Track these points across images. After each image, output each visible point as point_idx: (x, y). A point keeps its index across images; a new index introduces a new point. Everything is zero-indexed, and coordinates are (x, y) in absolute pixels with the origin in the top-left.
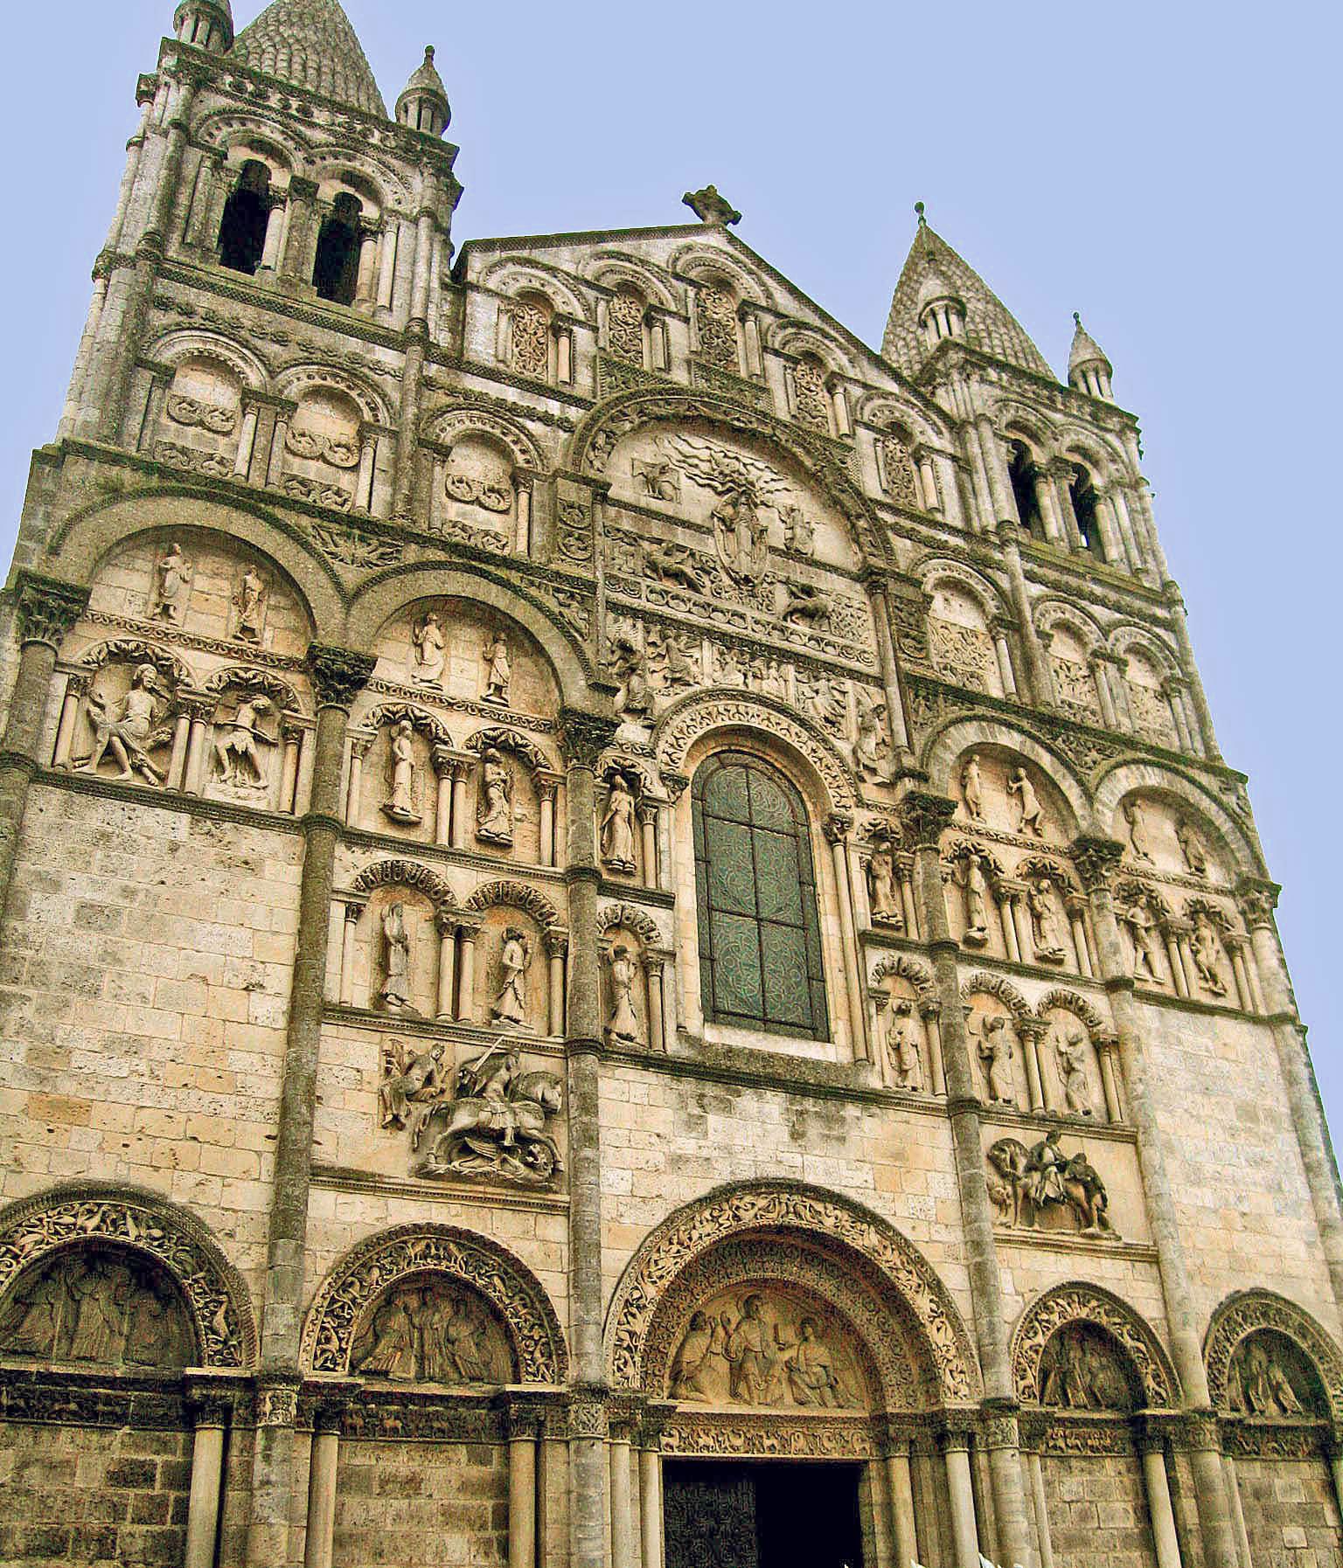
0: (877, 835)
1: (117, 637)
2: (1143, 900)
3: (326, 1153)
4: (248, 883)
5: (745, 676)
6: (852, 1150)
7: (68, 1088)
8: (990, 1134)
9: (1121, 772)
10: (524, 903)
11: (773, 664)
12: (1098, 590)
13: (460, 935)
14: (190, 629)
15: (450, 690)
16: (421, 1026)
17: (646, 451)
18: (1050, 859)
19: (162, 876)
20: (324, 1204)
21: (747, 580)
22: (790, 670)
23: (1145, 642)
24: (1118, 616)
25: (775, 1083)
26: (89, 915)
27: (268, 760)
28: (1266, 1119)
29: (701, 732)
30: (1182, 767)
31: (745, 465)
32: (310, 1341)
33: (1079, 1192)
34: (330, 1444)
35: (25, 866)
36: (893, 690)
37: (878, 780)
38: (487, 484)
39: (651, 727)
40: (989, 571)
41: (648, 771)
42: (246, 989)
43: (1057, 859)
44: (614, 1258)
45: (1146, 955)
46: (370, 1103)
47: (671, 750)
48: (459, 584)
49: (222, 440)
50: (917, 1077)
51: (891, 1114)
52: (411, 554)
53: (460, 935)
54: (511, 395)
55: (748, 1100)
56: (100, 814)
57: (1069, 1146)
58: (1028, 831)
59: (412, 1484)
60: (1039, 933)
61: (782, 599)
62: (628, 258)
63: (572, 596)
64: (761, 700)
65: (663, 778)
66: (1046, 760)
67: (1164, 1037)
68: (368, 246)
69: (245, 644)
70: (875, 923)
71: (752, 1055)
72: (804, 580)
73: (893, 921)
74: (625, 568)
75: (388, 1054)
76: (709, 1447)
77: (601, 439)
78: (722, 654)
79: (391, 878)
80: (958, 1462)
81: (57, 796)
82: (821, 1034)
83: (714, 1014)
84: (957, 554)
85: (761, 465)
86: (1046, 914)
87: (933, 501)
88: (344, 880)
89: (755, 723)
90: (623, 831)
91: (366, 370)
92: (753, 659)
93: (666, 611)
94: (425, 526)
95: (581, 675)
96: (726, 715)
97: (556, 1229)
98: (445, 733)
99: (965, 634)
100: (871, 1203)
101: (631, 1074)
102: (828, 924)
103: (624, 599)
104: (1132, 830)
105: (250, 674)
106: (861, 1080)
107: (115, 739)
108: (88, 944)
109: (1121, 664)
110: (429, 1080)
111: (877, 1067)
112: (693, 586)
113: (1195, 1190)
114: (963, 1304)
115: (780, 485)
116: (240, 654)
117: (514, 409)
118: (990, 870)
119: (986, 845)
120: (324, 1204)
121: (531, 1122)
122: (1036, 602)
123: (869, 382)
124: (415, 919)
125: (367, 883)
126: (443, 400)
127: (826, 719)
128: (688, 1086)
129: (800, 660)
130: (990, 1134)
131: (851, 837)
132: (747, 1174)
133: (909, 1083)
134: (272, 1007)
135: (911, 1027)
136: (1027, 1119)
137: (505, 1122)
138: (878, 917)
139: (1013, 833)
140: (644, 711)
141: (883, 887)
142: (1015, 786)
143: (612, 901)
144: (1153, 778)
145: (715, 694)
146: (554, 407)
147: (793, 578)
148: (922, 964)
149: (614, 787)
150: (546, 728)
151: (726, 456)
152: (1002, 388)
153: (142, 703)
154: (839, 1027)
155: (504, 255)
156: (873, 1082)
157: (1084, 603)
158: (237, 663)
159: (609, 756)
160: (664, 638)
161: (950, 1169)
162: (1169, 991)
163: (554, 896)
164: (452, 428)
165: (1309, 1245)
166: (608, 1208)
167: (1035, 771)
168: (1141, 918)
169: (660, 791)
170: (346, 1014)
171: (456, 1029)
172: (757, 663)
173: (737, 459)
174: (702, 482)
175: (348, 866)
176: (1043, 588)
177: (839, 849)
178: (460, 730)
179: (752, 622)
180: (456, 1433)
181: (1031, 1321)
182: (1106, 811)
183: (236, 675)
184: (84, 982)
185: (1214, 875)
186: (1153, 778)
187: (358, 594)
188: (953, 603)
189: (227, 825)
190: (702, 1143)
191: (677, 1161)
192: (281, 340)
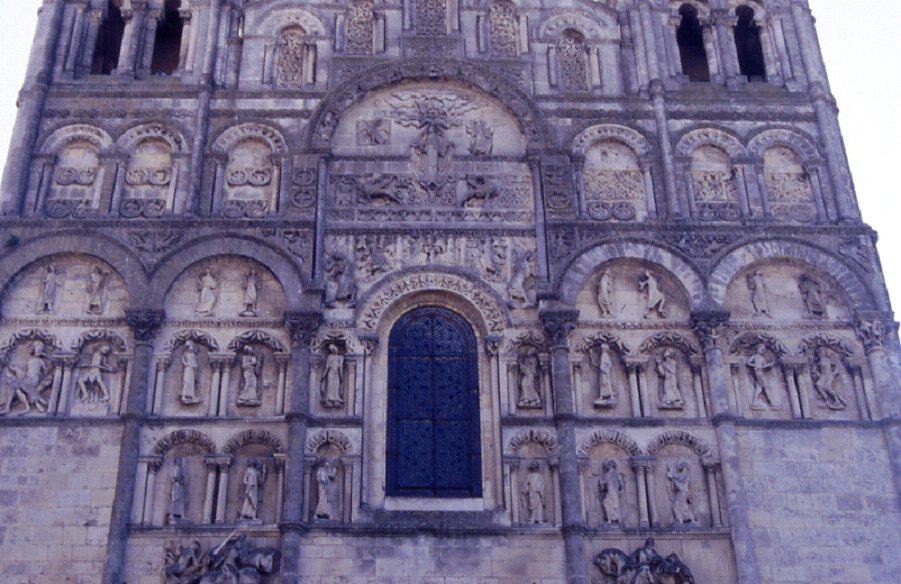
0: (524, 342)
1: (20, 330)
2: (762, 347)
4: (90, 461)
5: (429, 254)
6: (485, 568)
8: (592, 547)
9: (738, 253)
11: (450, 241)
13: (218, 469)
16: (189, 529)
17: (367, 113)
18: (673, 333)
19: (41, 466)
21: (433, 186)
22: (463, 241)
24: (760, 124)
28: (869, 506)
29: (391, 302)
31: (441, 101)
36: (541, 237)
37: (525, 305)
38: (255, 169)
39: (354, 307)
40: (639, 122)
41: (350, 338)
42: (87, 525)
43: (679, 331)
45: (763, 389)
47: (368, 319)
49: (88, 190)
50: (539, 513)
53: (218, 469)
54: (270, 104)
55: (407, 547)
57: (664, 547)
58: (654, 316)
60: (662, 390)
63: (297, 234)
64: (439, 269)
65: (361, 339)
66: (667, 259)
67: (768, 453)
68: (185, 27)
69: (95, 317)
70: (519, 408)
71: (412, 515)
72: (479, 173)
73: (533, 404)
74: (344, 202)
75: (168, 550)
78: (411, 243)
82: (475, 492)
83: (393, 489)
84: (611, 116)
85: (454, 97)
86: (668, 375)
87: (596, 81)
88: (148, 449)
89: (433, 287)
90: (334, 381)
91: (174, 118)
92: (435, 240)
93: (372, 224)
95: (300, 286)
96: (410, 285)
98: (216, 343)
102: (485, 415)
103: (342, 223)
104: (753, 295)
105: (97, 334)
106: (495, 521)
107: (19, 392)
109: (756, 161)
110: (191, 562)
111: (508, 511)
112: (391, 199)
113: (788, 569)
115: (465, 108)
116: (90, 322)
117: (272, 114)
118: (618, 351)
119: (615, 333)
122: (675, 138)
124: (195, 466)
125: (162, 449)
127: (488, 270)
128: (364, 542)
130: (592, 547)
131: (502, 351)
133: (533, 520)
134: (100, 533)
136: (628, 532)
138: (521, 404)
140: (349, 297)
141: (528, 382)
142: (642, 284)
143: (320, 429)
145: (406, 271)
146: (298, 104)
147: (470, 173)
148: (549, 433)
149: (330, 352)
150: (275, 325)
151: (426, 99)
154: (487, 486)
155: (270, 5)
156: (504, 521)
158: (89, 329)
159: (324, 334)
160: (368, 242)
161: (562, 576)
162: (785, 416)
163: (280, 433)
164: (224, 141)
168: (760, 362)
169: (358, 348)
170: (146, 529)
171: (214, 526)
172: (439, 243)
173: (435, 98)
174: (405, 123)
175: (152, 437)
176: (689, 121)
177: (493, 360)
178: (224, 339)
179: (438, 215)
182: (719, 287)
183: (89, 336)
185: (833, 313)
186: (771, 250)
187: (157, 267)
188: (610, 155)
189: (80, 429)
190: (372, 578)
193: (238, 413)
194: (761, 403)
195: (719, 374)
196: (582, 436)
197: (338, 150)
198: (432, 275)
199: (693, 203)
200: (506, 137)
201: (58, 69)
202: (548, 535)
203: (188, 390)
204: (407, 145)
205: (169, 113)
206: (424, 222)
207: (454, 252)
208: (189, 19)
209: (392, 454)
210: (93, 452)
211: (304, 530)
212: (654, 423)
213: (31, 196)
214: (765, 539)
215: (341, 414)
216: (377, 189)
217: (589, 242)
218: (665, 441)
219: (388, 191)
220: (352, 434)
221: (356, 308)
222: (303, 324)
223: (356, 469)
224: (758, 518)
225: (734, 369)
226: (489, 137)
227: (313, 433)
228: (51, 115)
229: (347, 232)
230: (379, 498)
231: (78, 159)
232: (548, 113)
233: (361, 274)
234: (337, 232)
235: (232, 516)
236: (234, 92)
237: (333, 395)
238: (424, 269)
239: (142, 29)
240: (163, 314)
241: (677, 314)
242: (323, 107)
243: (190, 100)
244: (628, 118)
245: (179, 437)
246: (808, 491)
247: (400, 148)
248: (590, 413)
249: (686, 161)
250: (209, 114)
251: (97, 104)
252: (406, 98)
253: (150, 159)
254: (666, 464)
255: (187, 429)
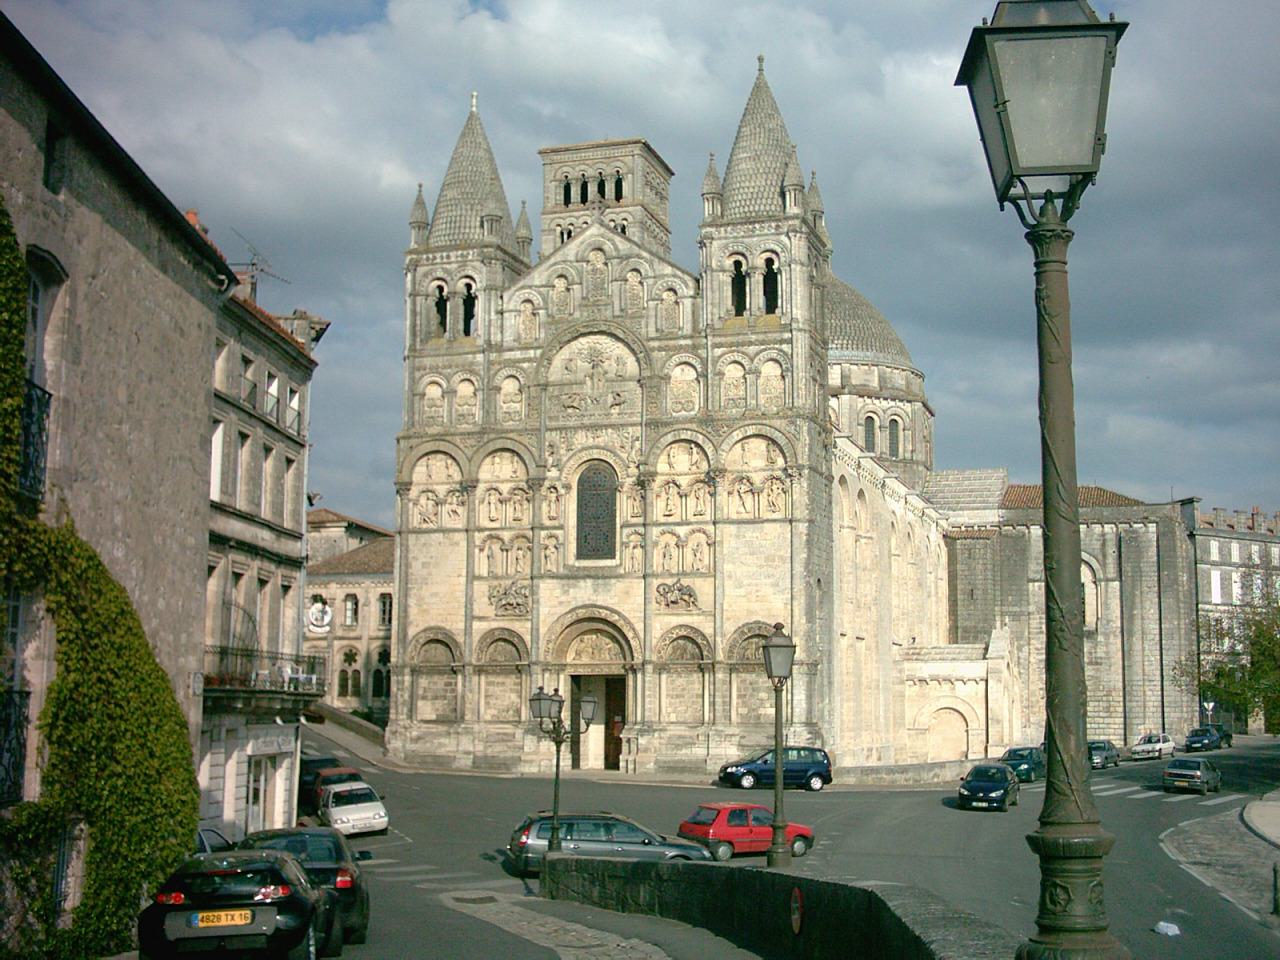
1: (422, 488)
3: (476, 612)
7: (425, 606)
8: (656, 582)
9: (735, 433)
10: (524, 537)
12: (753, 337)
14: (437, 480)
15: (502, 477)
16: (496, 577)
17: (565, 353)
20: (476, 625)
22: (610, 430)
23: (775, 356)
25: (589, 577)
26: (425, 565)
27: (460, 510)
30: (767, 422)
32: (475, 656)
33: (686, 597)
34: (483, 678)
35: (410, 556)
41: (558, 485)
44: (543, 630)
46: (486, 600)
48: (499, 444)
51: (627, 580)
52: (486, 437)
54: (518, 355)
55: (582, 583)
56: (423, 538)
57: (685, 582)
58: (694, 468)
59: (503, 683)
61: (610, 400)
62: (555, 264)
64: (597, 447)
66: (700, 439)
67: (737, 536)
71: (585, 568)
72: (618, 390)
76: (581, 671)
77: (545, 363)
79: (491, 537)
80: (639, 676)
81: (414, 536)
82: (614, 557)
88: (478, 542)
89: (596, 456)
90: (553, 506)
94: (493, 420)
97: (529, 625)
99: (688, 383)
100: (616, 608)
101: (549, 581)
103: (554, 424)
108: (425, 572)
109: (757, 373)
114: (642, 635)
119: (676, 478)
120: (476, 625)
121: (520, 601)
123: (657, 273)
124: (496, 547)
125: (485, 541)
126: (497, 367)
128: (564, 582)
129: (611, 426)
130: (656, 582)
131: (625, 489)
132: (580, 604)
134: (463, 580)
135: (639, 552)
136: (672, 575)
137: (513, 601)
139: (686, 470)
141: (637, 504)
144: (751, 431)
146: (531, 353)
148: (641, 530)
152: (726, 238)
153: (431, 503)
156: (622, 571)
157: (744, 349)
159: (547, 484)
163: (530, 534)
164: (497, 381)
165: (786, 604)
166: (542, 618)
167: (697, 445)
170: (480, 578)
175: (478, 537)
178: (505, 488)
180: (511, 673)
181: (663, 638)
184: (425, 581)
191: (561, 603)
192: (450, 367)
193: (514, 524)
194: (742, 509)
195: (722, 497)
196: (656, 531)
197: (552, 379)
198: (595, 451)
199: (723, 399)
200: (631, 366)
201: (418, 340)
202: (638, 578)
203: (493, 514)
204: (583, 375)
205: (472, 363)
206: (593, 420)
207: (606, 437)
208: (476, 297)
209: (578, 539)
210: (457, 544)
211: (542, 577)
212: (688, 523)
213: (417, 417)
214: (730, 577)
215: (556, 523)
216: (568, 402)
217: (666, 430)
218: (694, 531)
219: (575, 404)
220: (559, 533)
221: (560, 470)
222: (534, 484)
223: (561, 550)
224: (728, 567)
225: (730, 493)
226: (624, 364)
227: (543, 533)
228: (419, 370)
229: (556, 429)
230: (572, 560)
231: (434, 392)
232: (653, 349)
233: (562, 452)
234: (551, 430)
235: (513, 570)
236: (500, 348)
237: (553, 514)
238: (591, 448)
239: (456, 306)
240: (477, 481)
241: (704, 466)
242: (542, 355)
243: (482, 355)
244: (695, 348)
245: (491, 537)
246: (752, 554)
247: (580, 376)
248: (663, 520)
249: (721, 374)
250: (491, 363)
251: (440, 361)
252: (584, 342)
253: (465, 390)
254: (692, 544)
255: (493, 533)
